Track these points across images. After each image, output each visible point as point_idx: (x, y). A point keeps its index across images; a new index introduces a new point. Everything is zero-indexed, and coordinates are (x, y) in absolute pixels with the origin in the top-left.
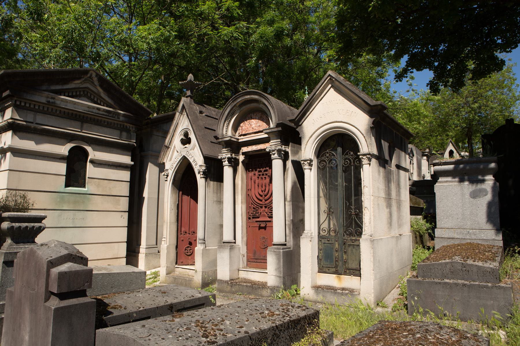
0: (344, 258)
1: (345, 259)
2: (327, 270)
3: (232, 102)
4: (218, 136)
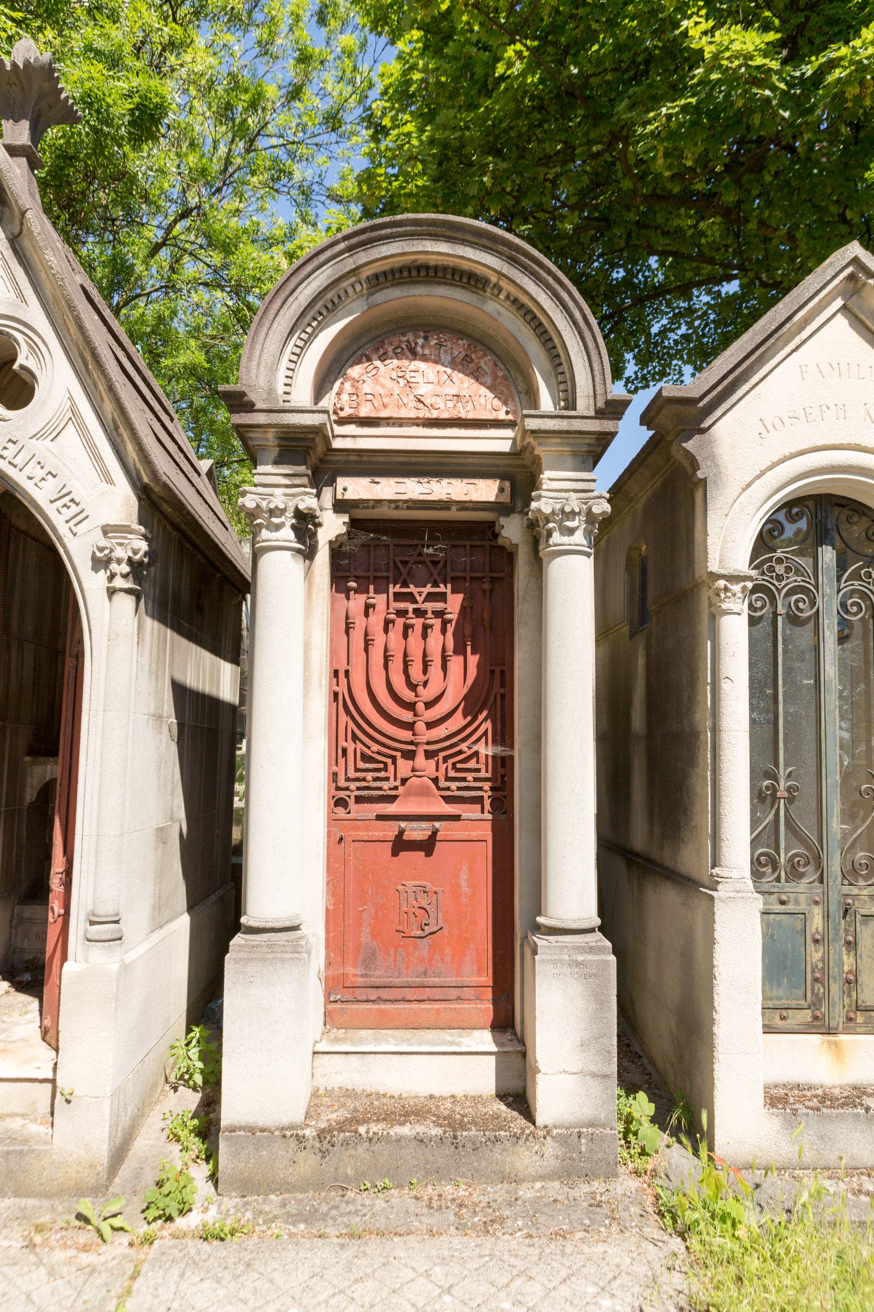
0: (846, 969)
1: (850, 972)
2: (777, 1020)
3: (350, 249)
4: (252, 397)
